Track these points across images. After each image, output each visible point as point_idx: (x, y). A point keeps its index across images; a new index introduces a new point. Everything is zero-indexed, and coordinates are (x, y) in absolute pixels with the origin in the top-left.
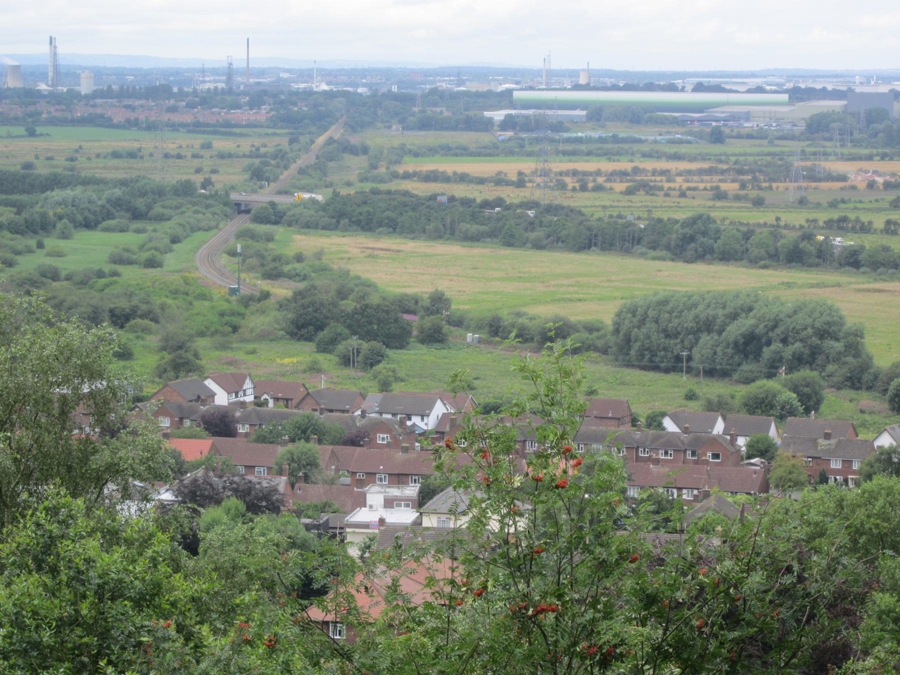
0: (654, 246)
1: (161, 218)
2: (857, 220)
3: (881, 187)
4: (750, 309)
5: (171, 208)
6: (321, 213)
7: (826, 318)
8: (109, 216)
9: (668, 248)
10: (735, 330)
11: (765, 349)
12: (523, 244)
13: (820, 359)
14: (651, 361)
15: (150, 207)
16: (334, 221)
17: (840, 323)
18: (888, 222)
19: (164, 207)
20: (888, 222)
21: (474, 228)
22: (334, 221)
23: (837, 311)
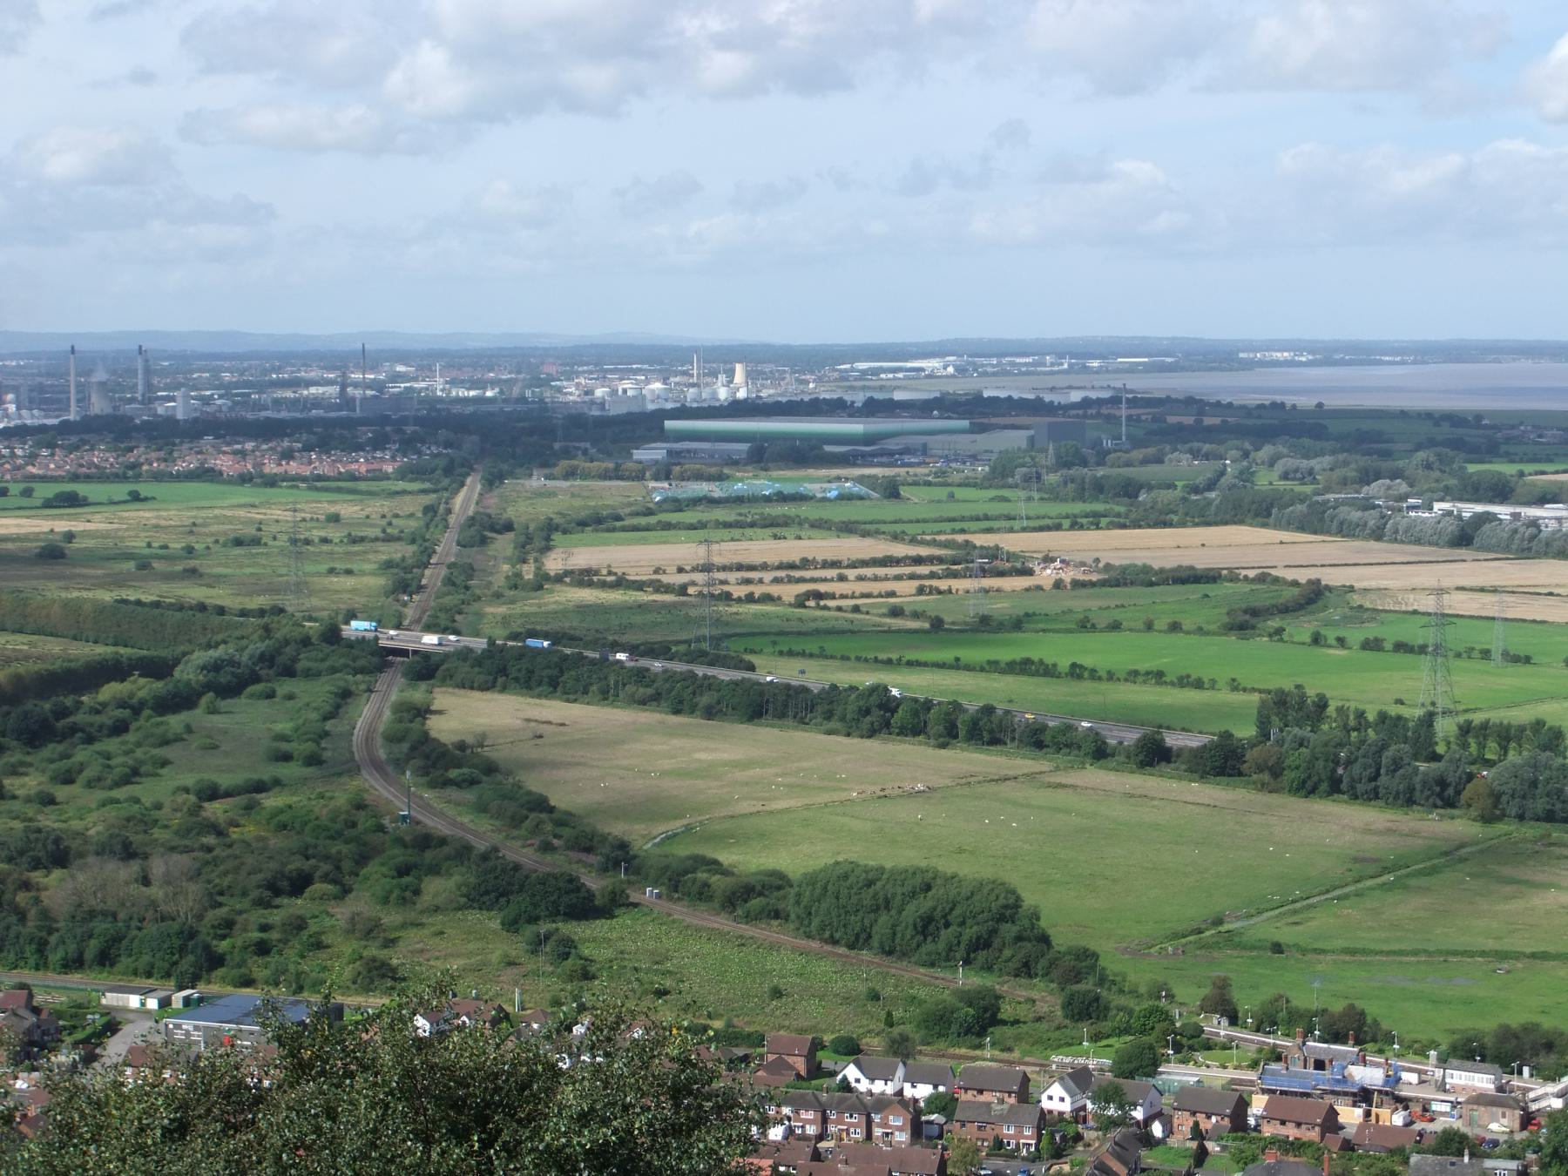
0: (829, 716)
1: (309, 674)
2: (1041, 662)
3: (1069, 587)
4: (928, 888)
5: (316, 660)
6: (477, 669)
7: (1002, 901)
8: (256, 679)
9: (843, 719)
10: (914, 910)
11: (943, 932)
12: (692, 711)
13: (997, 942)
14: (832, 936)
15: (295, 660)
16: (491, 678)
17: (1017, 904)
18: (1074, 665)
19: (308, 659)
20: (1074, 665)
21: (642, 691)
22: (491, 678)
23: (1014, 892)
